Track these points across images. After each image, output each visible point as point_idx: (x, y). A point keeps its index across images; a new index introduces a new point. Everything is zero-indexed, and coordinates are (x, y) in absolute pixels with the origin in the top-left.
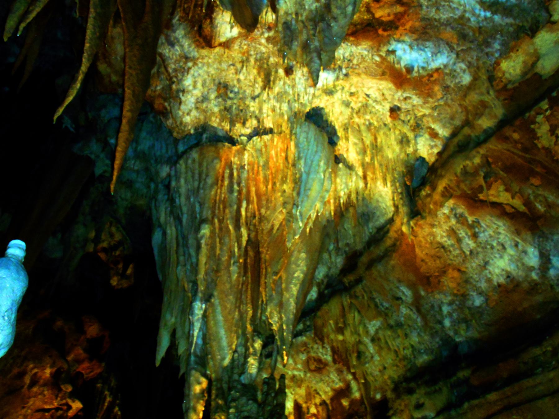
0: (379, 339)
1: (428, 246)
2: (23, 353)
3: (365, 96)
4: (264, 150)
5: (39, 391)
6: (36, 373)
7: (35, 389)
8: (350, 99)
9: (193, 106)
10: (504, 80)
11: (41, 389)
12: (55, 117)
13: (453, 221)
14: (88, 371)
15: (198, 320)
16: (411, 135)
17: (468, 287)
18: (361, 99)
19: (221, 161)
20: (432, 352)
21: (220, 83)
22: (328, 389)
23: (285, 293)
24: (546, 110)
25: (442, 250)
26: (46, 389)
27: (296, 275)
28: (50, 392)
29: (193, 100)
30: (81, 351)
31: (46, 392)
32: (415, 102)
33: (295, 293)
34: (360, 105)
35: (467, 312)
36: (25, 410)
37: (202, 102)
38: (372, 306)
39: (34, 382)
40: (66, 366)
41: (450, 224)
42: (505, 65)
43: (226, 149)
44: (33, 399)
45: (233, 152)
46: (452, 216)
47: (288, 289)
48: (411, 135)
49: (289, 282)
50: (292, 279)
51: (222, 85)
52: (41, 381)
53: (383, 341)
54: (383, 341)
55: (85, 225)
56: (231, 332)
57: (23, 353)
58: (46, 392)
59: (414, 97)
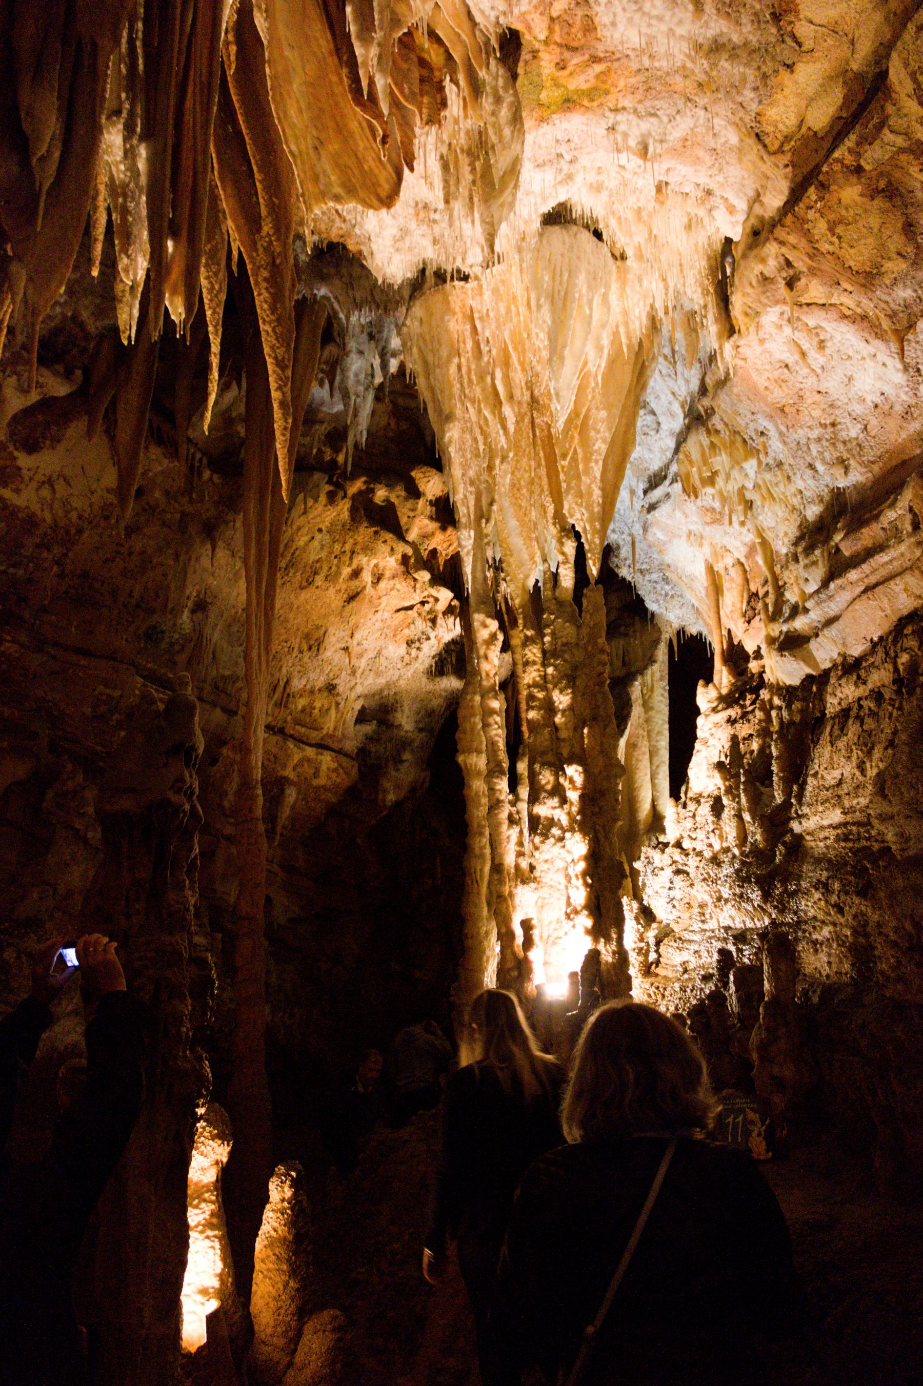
0: (759, 487)
1: (767, 367)
2: (348, 547)
3: (618, 169)
4: (502, 289)
5: (389, 587)
6: (376, 566)
7: (383, 585)
8: (600, 178)
9: (392, 250)
10: (779, 136)
11: (392, 582)
12: (206, 428)
13: (788, 330)
14: (445, 546)
15: (468, 553)
16: (701, 212)
17: (837, 412)
18: (613, 174)
19: (454, 314)
20: (821, 501)
21: (417, 204)
22: (738, 544)
23: (583, 478)
24: (816, 202)
25: (786, 371)
26: (396, 581)
27: (596, 447)
28: (404, 583)
29: (389, 242)
30: (427, 521)
31: (398, 586)
32: (683, 173)
33: (598, 475)
34: (616, 182)
35: (840, 446)
36: (380, 613)
37: (402, 238)
38: (739, 444)
39: (378, 578)
40: (409, 551)
41: (785, 335)
42: (772, 113)
43: (456, 291)
44: (384, 599)
45: (470, 292)
46: (784, 323)
47: (587, 471)
48: (701, 212)
49: (587, 460)
50: (592, 455)
51: (420, 206)
52: (388, 574)
53: (763, 487)
54: (763, 487)
55: (361, 353)
56: (531, 539)
57: (348, 547)
58: (398, 586)
59: (678, 166)
